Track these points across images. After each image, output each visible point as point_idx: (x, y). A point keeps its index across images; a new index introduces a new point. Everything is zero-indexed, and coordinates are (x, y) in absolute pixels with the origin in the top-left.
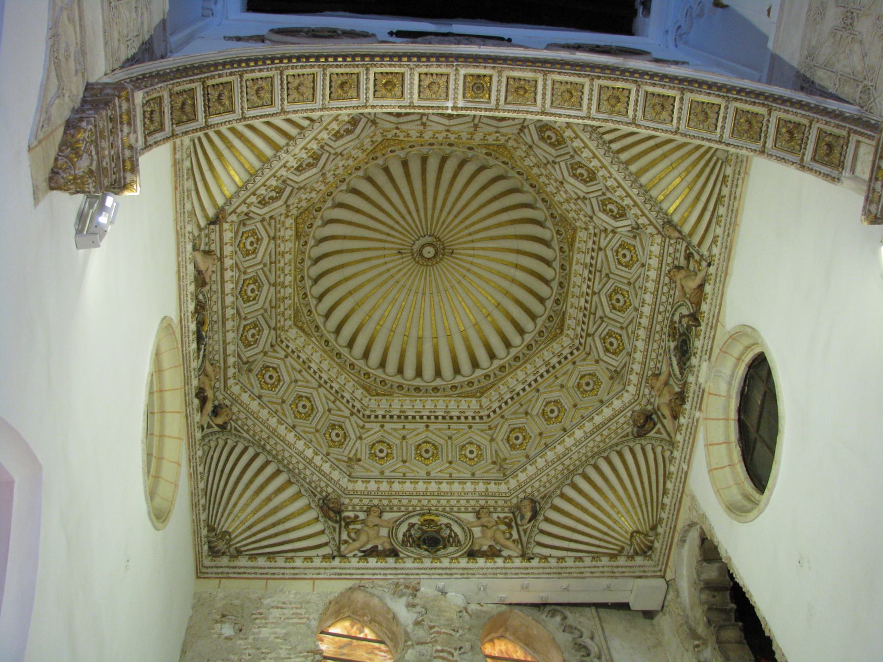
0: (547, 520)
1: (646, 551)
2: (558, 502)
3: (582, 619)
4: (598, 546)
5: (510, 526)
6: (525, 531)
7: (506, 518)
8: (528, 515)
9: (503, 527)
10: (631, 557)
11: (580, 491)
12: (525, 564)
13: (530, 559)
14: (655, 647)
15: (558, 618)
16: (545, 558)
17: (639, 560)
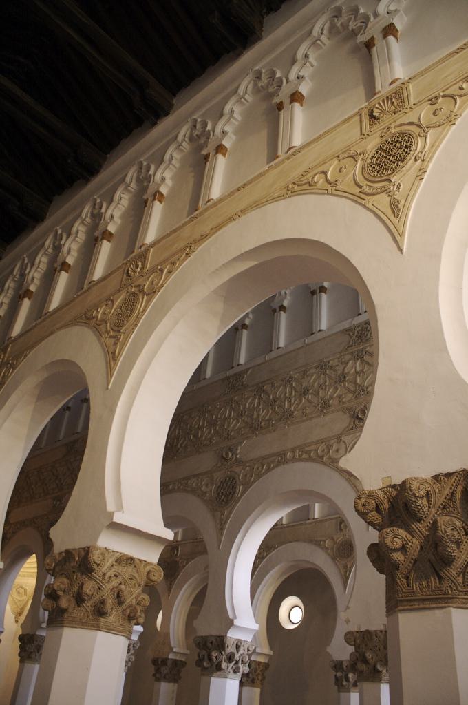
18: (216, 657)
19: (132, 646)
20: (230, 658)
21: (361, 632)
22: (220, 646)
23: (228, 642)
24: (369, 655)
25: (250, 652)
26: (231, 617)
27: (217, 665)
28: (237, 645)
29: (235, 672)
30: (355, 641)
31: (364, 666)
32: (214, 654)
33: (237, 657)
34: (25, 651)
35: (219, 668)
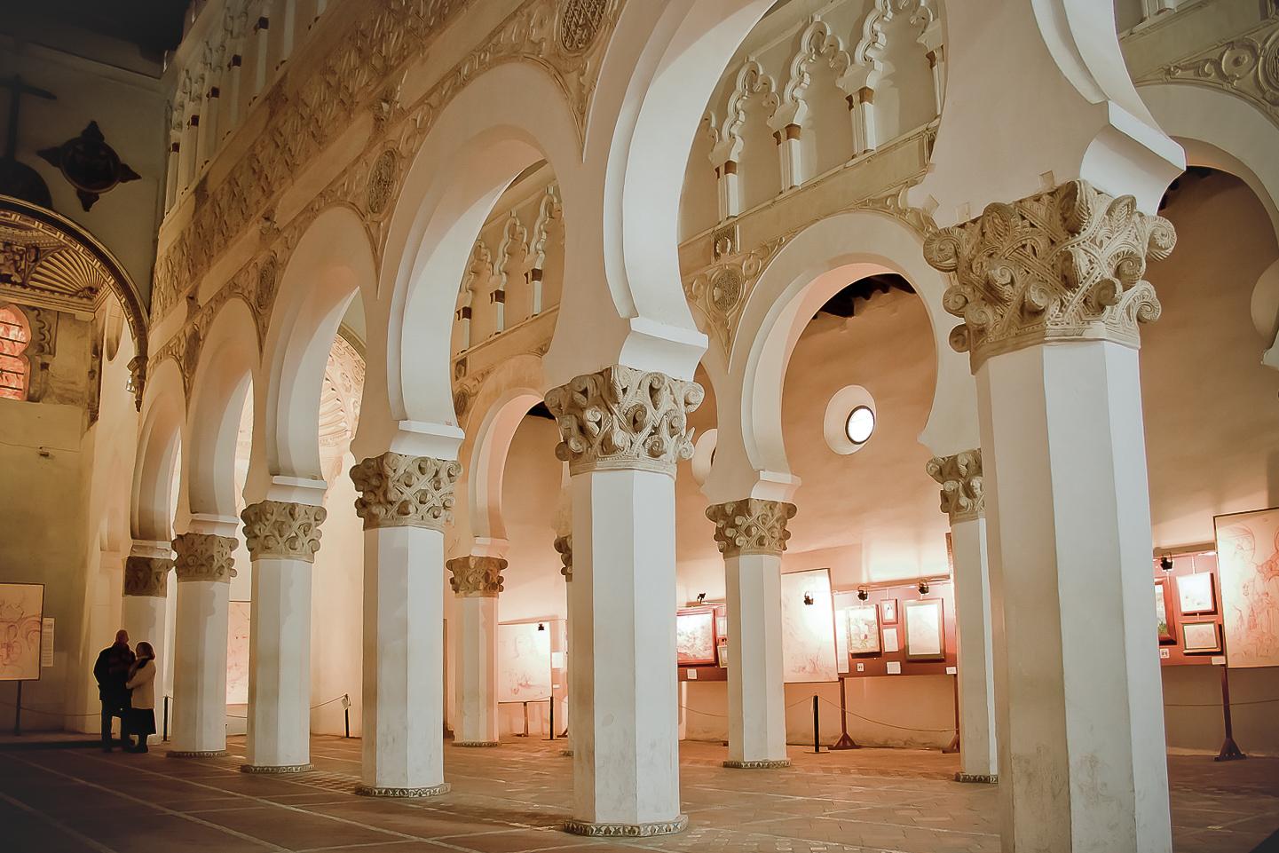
0: (41, 266)
1: (90, 299)
2: (50, 258)
3: (49, 317)
4: (67, 285)
5: (21, 259)
6: (29, 266)
7: (22, 250)
8: (33, 258)
9: (17, 258)
10: (81, 298)
11: (63, 256)
12: (23, 290)
13: (25, 287)
14: (83, 336)
15: (36, 312)
16: (34, 288)
17: (85, 300)
18: (599, 424)
19: (443, 475)
20: (635, 424)
21: (974, 221)
22: (605, 395)
23: (620, 380)
24: (1000, 276)
25: (693, 409)
26: (623, 312)
27: (602, 444)
28: (651, 388)
29: (654, 454)
30: (956, 253)
31: (989, 311)
32: (591, 416)
33: (652, 417)
34: (256, 537)
35: (607, 447)
